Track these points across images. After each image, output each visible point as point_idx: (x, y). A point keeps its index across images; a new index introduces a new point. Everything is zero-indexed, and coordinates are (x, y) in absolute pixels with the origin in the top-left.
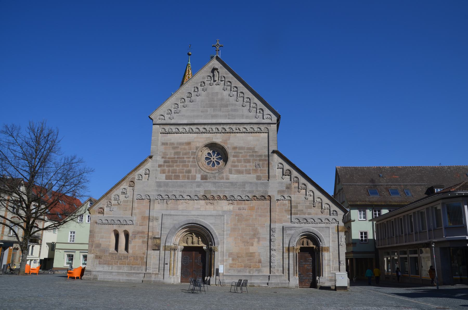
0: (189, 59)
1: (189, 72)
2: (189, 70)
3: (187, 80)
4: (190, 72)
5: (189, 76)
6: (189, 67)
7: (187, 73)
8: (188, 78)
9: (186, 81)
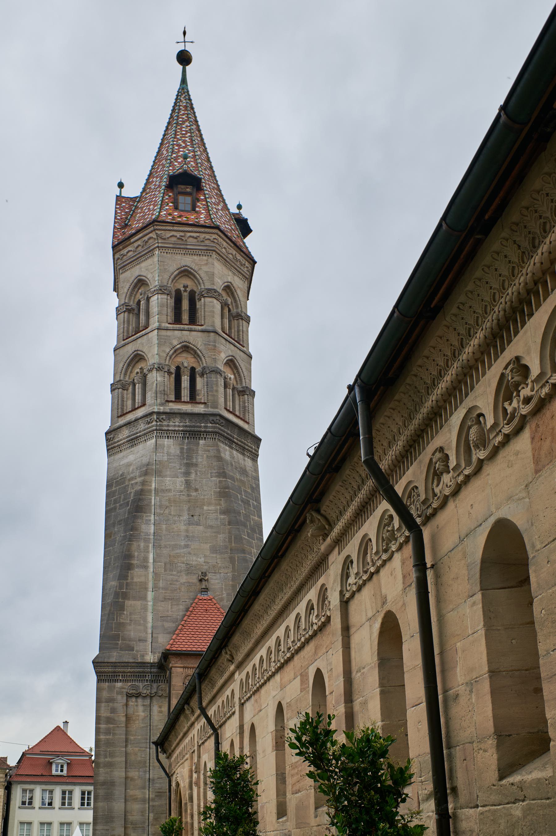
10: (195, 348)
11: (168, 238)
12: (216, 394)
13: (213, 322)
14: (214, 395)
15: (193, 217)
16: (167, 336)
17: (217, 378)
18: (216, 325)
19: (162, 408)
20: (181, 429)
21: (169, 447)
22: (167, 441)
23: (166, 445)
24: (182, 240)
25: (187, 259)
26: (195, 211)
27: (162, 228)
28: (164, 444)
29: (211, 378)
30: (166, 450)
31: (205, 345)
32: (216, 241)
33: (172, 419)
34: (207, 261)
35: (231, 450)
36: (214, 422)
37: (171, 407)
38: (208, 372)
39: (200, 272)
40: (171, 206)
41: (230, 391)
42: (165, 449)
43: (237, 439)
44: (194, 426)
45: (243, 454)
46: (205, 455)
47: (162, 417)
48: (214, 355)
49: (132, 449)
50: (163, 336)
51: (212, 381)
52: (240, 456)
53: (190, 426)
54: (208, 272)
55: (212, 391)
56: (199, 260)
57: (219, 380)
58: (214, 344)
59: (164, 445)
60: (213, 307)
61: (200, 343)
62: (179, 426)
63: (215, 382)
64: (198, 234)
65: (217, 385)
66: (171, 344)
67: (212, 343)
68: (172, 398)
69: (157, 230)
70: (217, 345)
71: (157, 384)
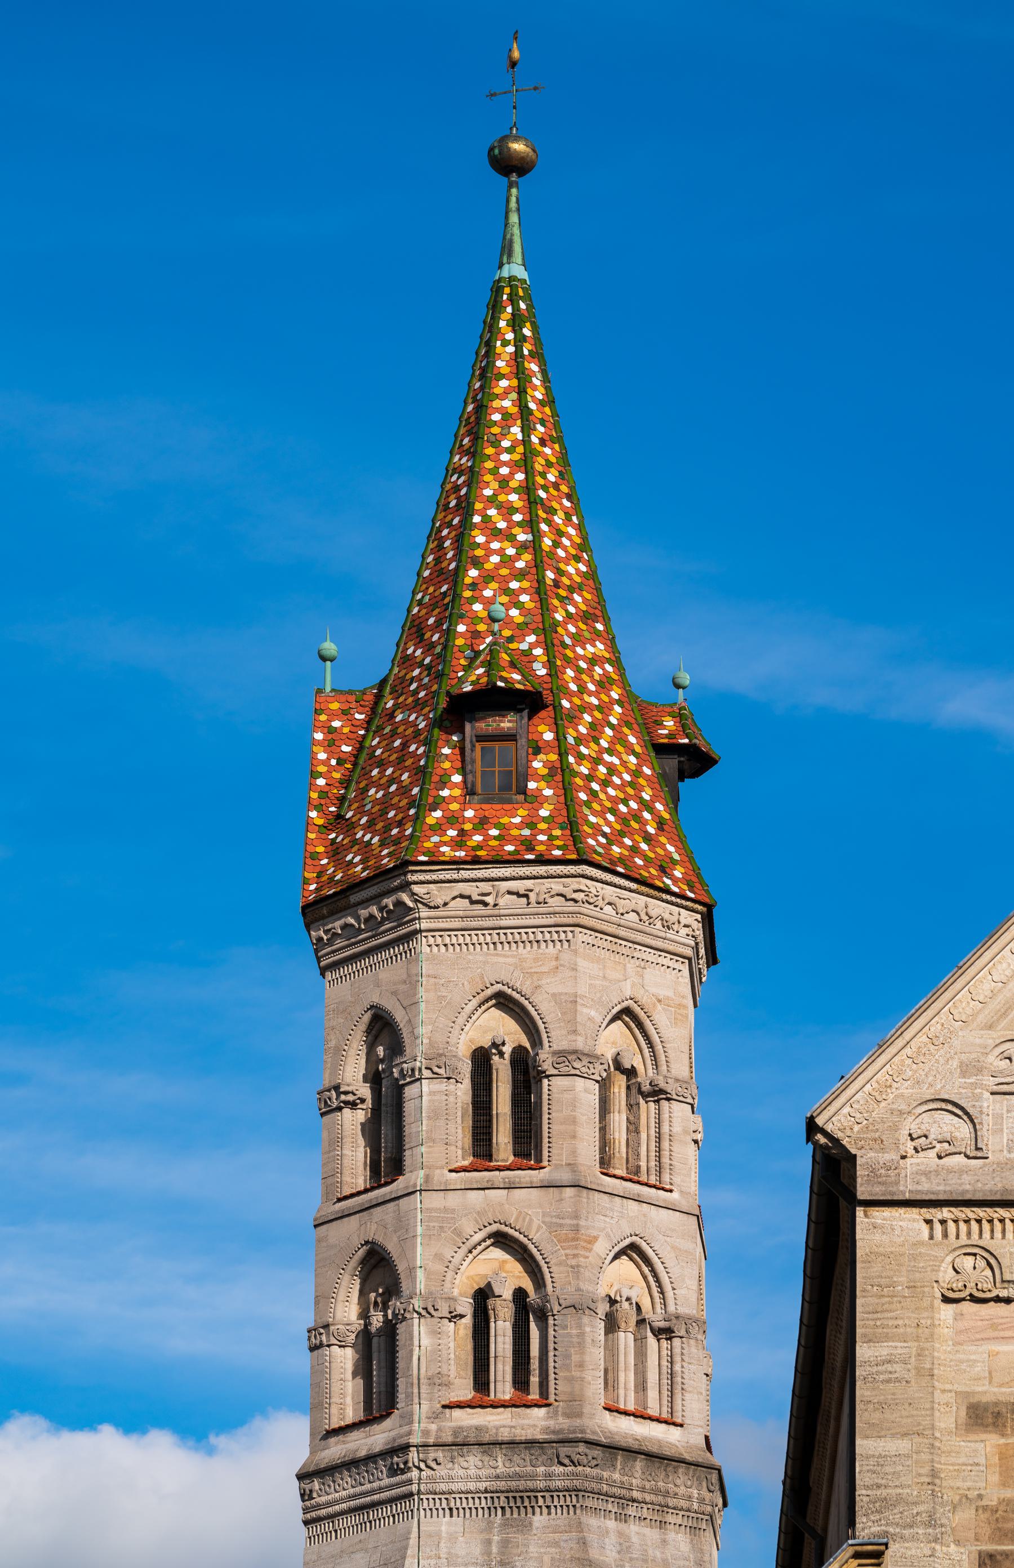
0: (514, 218)
1: (521, 391)
2: (518, 354)
3: (504, 483)
4: (536, 382)
5: (526, 442)
6: (516, 322)
7: (507, 403)
8: (514, 465)
9: (491, 501)
10: (521, 1238)
11: (445, 904)
12: (578, 1374)
13: (574, 1153)
14: (571, 1380)
15: (517, 820)
16: (446, 1210)
17: (580, 1326)
18: (581, 1160)
19: (433, 1427)
20: (482, 1486)
21: (452, 1538)
22: (449, 1524)
23: (444, 1535)
24: (486, 904)
25: (501, 960)
26: (525, 793)
27: (428, 877)
28: (441, 1531)
29: (565, 1327)
30: (445, 1550)
31: (549, 1225)
32: (580, 896)
33: (461, 1459)
34: (557, 959)
35: (622, 1526)
36: (572, 1461)
37: (459, 1424)
38: (556, 1308)
39: (536, 999)
40: (456, 785)
41: (626, 1339)
42: (442, 1545)
43: (643, 1490)
44: (518, 1476)
45: (662, 1524)
46: (547, 1559)
47: (432, 1455)
48: (575, 1256)
49: (363, 1536)
50: (437, 1210)
51: (570, 1335)
52: (652, 1534)
53: (509, 1477)
54: (561, 994)
55: (567, 1367)
56: (536, 960)
57: (588, 1329)
58: (575, 1222)
59: (438, 1534)
60: (573, 1104)
61: (536, 1222)
62: (479, 1479)
63: (575, 1340)
64: (529, 884)
65: (581, 1345)
66: (458, 1232)
67: (568, 1221)
68: (465, 1391)
69: (416, 883)
70: (582, 1223)
71: (419, 1359)
